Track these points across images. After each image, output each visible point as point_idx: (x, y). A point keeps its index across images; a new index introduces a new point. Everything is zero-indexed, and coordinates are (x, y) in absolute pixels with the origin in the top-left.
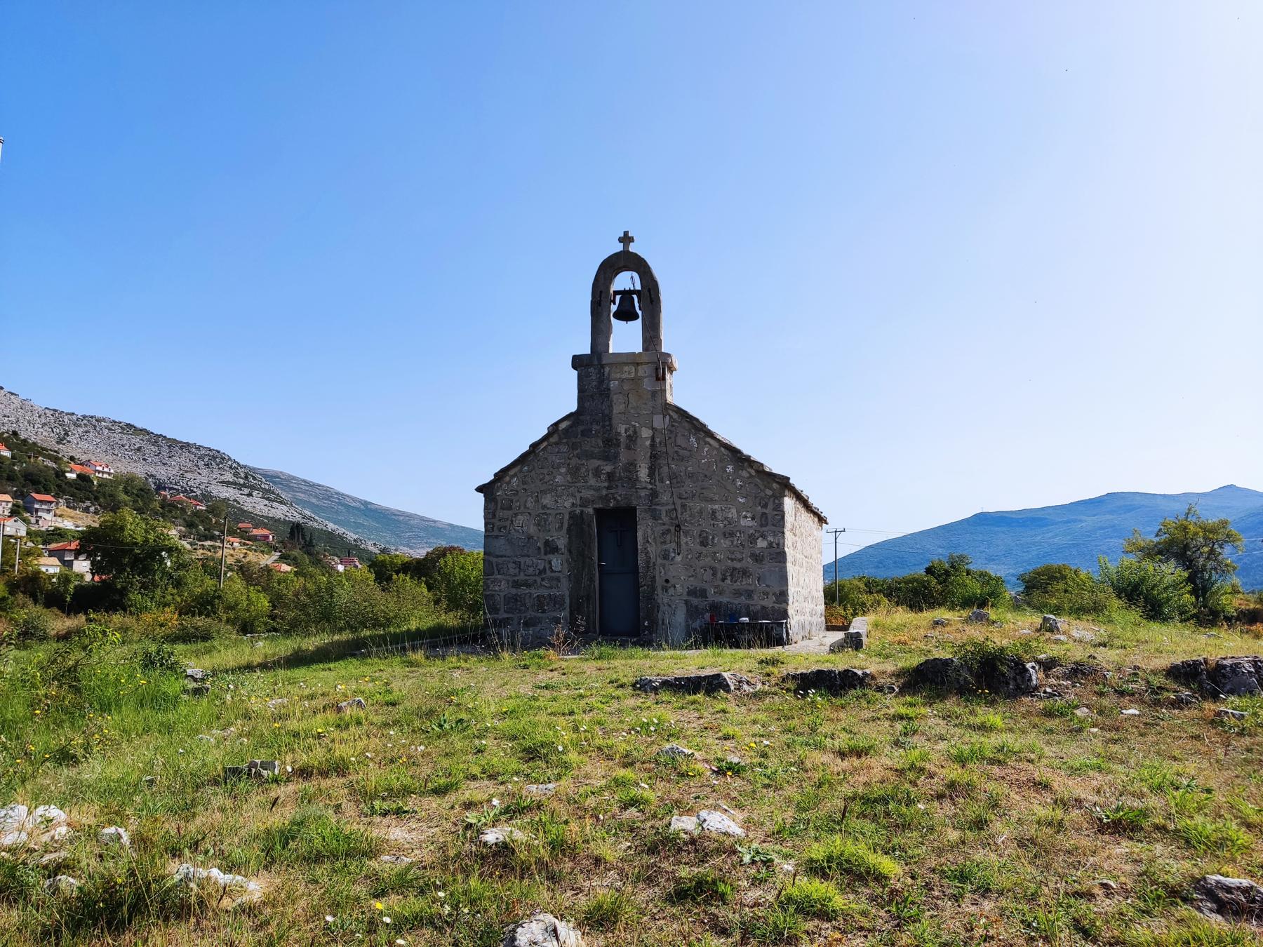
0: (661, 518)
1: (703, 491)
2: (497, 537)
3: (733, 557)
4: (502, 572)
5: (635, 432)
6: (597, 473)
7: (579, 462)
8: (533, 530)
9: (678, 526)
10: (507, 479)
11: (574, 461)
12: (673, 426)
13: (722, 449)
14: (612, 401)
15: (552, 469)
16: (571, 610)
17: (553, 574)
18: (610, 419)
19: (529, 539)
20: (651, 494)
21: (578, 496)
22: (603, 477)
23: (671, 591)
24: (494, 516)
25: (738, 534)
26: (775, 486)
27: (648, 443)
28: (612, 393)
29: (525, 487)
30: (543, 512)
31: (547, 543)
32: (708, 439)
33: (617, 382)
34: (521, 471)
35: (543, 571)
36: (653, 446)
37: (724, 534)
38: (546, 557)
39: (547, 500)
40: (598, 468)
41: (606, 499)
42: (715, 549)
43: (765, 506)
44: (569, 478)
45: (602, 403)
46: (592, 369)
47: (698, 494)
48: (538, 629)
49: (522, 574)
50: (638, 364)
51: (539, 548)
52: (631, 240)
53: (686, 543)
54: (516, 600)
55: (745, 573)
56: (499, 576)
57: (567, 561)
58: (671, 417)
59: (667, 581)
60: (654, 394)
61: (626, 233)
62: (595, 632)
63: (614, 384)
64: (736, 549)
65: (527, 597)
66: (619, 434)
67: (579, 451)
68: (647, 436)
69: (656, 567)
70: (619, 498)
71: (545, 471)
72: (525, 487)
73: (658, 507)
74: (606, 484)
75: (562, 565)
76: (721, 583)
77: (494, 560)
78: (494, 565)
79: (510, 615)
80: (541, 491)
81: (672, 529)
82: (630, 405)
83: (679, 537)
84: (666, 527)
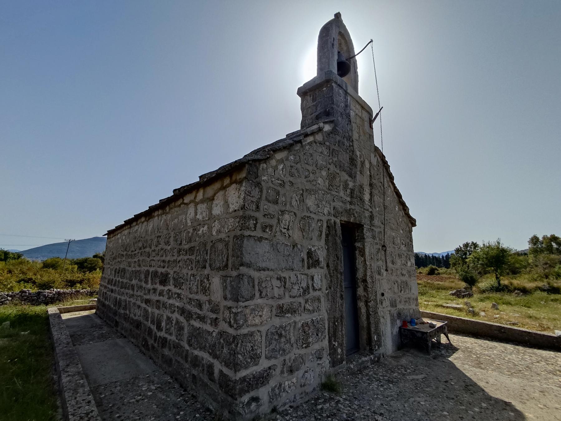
2: (260, 239)
8: (296, 235)
15: (315, 169)
19: (294, 246)
21: (333, 204)
22: (349, 191)
38: (307, 271)
41: (349, 212)
48: (300, 373)
54: (280, 336)
56: (260, 301)
57: (326, 276)
78: (256, 283)
80: (307, 190)
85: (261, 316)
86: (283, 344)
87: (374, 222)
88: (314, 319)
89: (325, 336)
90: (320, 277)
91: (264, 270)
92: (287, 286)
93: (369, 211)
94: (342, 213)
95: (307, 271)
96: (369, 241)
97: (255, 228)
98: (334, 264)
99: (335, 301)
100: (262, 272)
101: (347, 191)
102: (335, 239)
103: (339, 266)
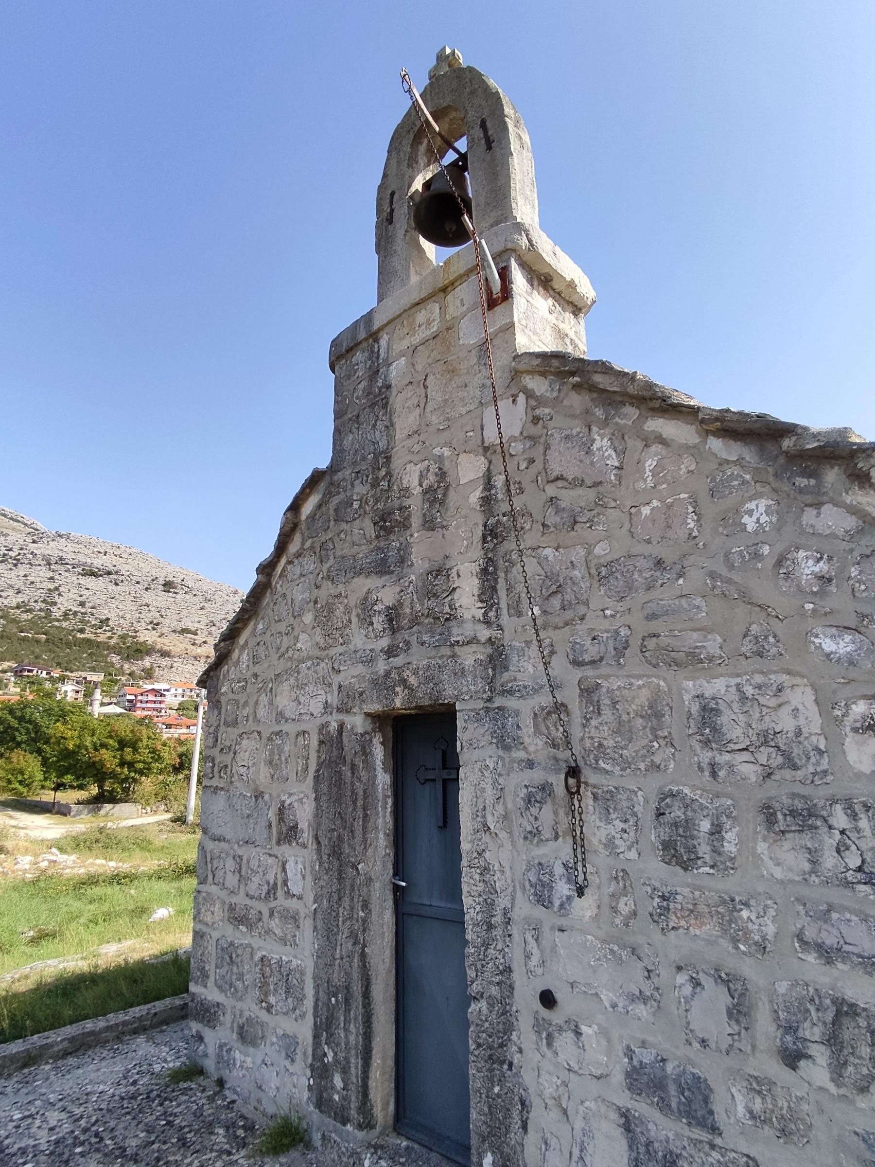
0: (518, 743)
1: (654, 626)
3: (830, 940)
5: (442, 475)
8: (263, 774)
9: (573, 772)
10: (235, 655)
11: (328, 589)
12: (536, 420)
13: (715, 444)
16: (315, 1023)
18: (388, 459)
19: (256, 797)
20: (491, 658)
21: (336, 679)
22: (379, 622)
23: (565, 1041)
27: (475, 496)
28: (394, 391)
29: (257, 669)
30: (277, 728)
32: (657, 425)
34: (253, 633)
36: (487, 501)
37: (769, 814)
38: (277, 850)
39: (284, 701)
40: (366, 599)
42: (731, 884)
45: (374, 426)
46: (359, 356)
47: (635, 643)
50: (444, 290)
53: (610, 844)
58: (529, 394)
59: (548, 999)
60: (483, 349)
62: (367, 1124)
63: (397, 371)
64: (837, 895)
65: (247, 956)
66: (405, 492)
67: (331, 561)
68: (472, 476)
69: (515, 930)
70: (413, 680)
71: (282, 627)
72: (257, 669)
73: (511, 703)
74: (385, 642)
75: (304, 877)
76: (775, 1069)
78: (209, 859)
81: (558, 781)
82: (429, 408)
83: (575, 814)
84: (537, 776)
85: (213, 913)
86: (234, 977)
87: (506, 676)
88: (284, 958)
89: (305, 1014)
90: (300, 866)
91: (219, 840)
92: (243, 873)
93: (478, 642)
94: (361, 694)
96: (474, 758)
97: (212, 772)
98: (330, 839)
99: (333, 939)
100: (216, 842)
101: (372, 624)
102: (340, 773)
103: (346, 845)
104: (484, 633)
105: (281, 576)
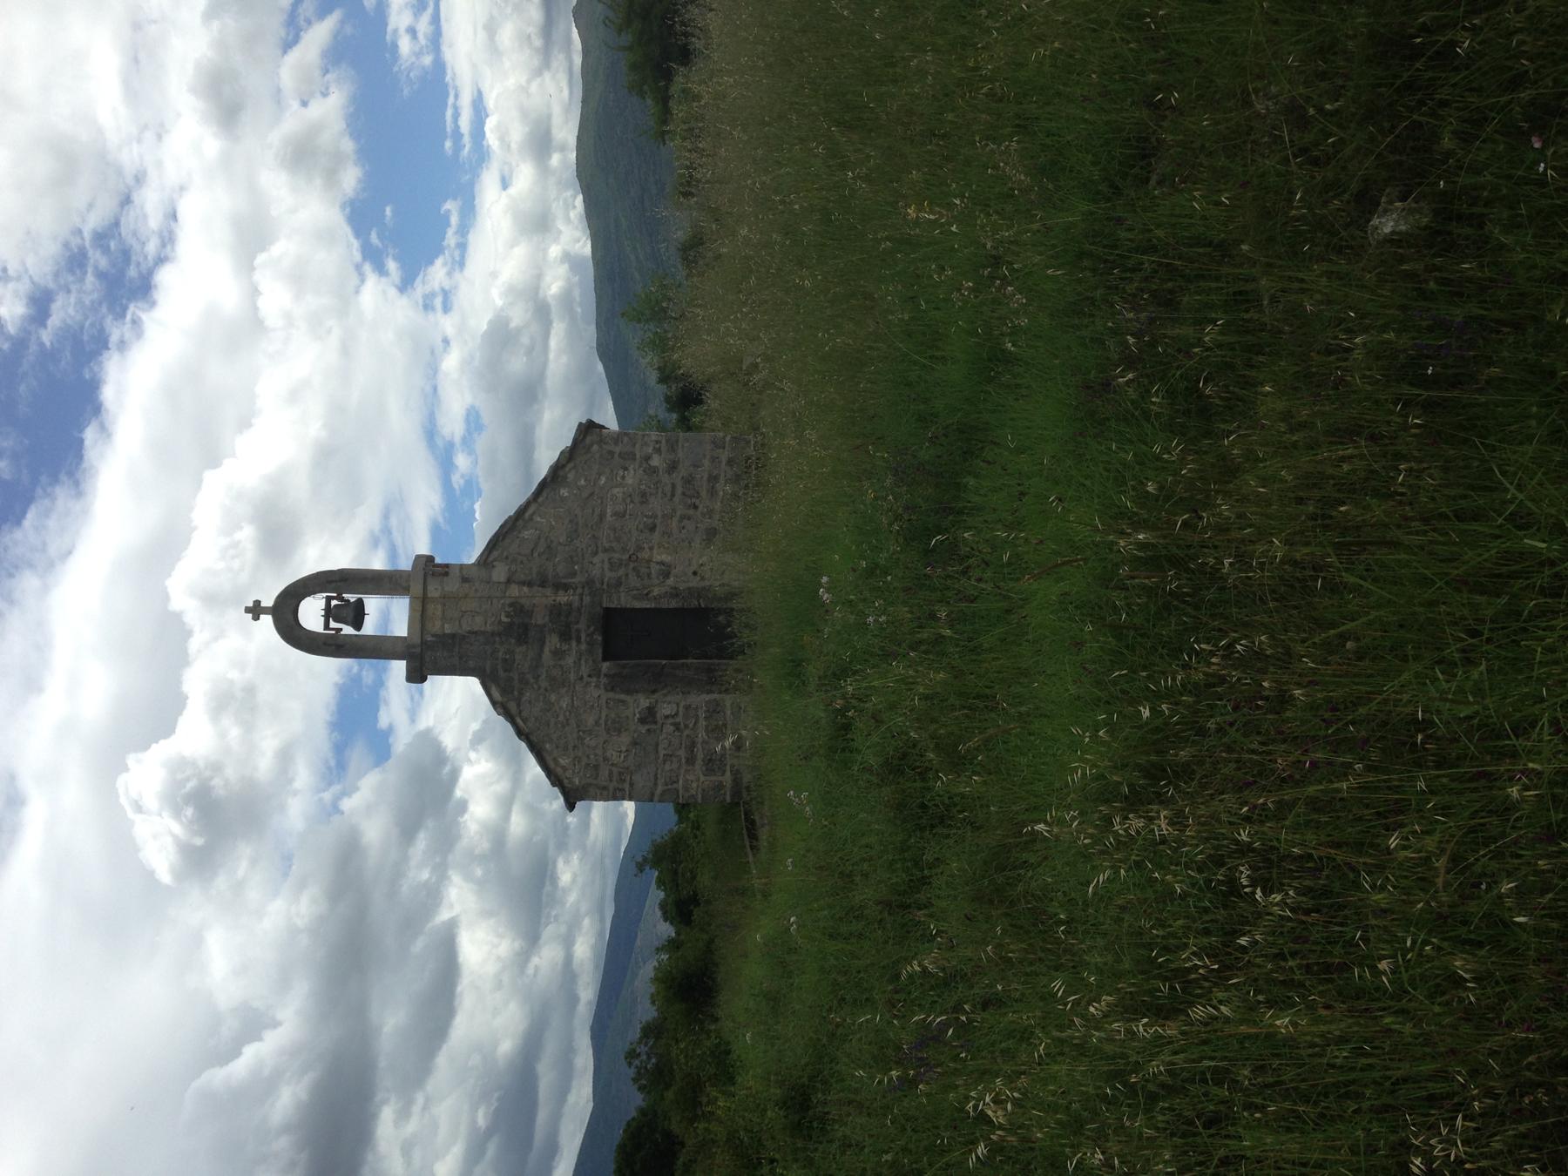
0: (620, 578)
2: (632, 785)
4: (675, 779)
6: (558, 654)
7: (544, 676)
8: (625, 739)
10: (559, 770)
12: (507, 558)
13: (540, 500)
14: (469, 632)
17: (681, 713)
21: (586, 679)
24: (605, 788)
25: (643, 487)
26: (588, 440)
27: (525, 589)
29: (570, 748)
31: (642, 721)
32: (527, 515)
33: (446, 626)
35: (677, 726)
36: (530, 584)
43: (611, 453)
44: (563, 691)
49: (679, 753)
51: (649, 730)
52: (257, 603)
54: (710, 760)
55: (688, 481)
56: (681, 782)
58: (495, 560)
61: (248, 610)
63: (448, 629)
64: (660, 490)
68: (517, 591)
71: (553, 720)
74: (574, 644)
77: (660, 789)
79: (728, 767)
80: (578, 726)
82: (478, 610)
95: (659, 726)
104: (579, 591)
105: (525, 723)
